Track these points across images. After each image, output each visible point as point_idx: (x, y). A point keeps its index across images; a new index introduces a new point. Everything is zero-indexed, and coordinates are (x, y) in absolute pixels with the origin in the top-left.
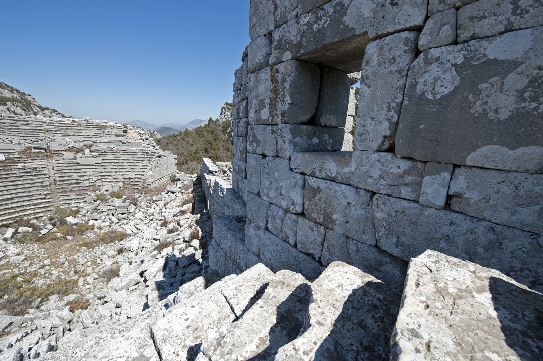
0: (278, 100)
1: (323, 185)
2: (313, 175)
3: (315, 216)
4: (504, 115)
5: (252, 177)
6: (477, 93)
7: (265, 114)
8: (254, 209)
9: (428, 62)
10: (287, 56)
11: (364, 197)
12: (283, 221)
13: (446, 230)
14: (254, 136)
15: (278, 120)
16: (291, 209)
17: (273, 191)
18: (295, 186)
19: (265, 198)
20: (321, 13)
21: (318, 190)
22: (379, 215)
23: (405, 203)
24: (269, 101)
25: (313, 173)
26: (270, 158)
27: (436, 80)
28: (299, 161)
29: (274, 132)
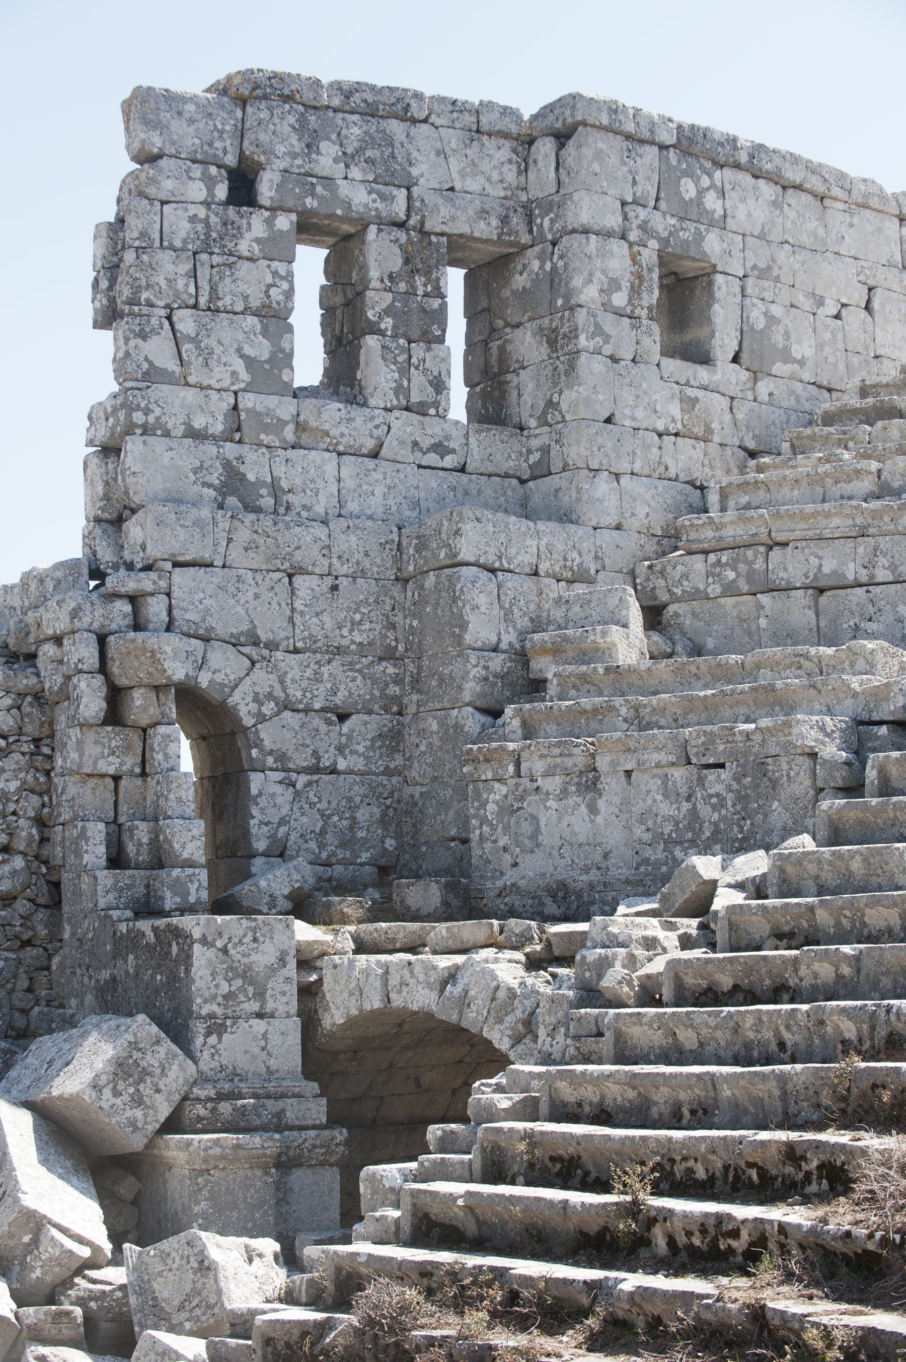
1: (700, 394)
2: (688, 384)
4: (781, 346)
5: (598, 392)
7: (620, 299)
8: (609, 445)
10: (653, 244)
12: (660, 448)
14: (597, 325)
15: (637, 312)
17: (641, 408)
18: (672, 398)
19: (627, 423)
21: (696, 400)
22: (740, 416)
25: (688, 381)
28: (671, 368)
29: (633, 327)
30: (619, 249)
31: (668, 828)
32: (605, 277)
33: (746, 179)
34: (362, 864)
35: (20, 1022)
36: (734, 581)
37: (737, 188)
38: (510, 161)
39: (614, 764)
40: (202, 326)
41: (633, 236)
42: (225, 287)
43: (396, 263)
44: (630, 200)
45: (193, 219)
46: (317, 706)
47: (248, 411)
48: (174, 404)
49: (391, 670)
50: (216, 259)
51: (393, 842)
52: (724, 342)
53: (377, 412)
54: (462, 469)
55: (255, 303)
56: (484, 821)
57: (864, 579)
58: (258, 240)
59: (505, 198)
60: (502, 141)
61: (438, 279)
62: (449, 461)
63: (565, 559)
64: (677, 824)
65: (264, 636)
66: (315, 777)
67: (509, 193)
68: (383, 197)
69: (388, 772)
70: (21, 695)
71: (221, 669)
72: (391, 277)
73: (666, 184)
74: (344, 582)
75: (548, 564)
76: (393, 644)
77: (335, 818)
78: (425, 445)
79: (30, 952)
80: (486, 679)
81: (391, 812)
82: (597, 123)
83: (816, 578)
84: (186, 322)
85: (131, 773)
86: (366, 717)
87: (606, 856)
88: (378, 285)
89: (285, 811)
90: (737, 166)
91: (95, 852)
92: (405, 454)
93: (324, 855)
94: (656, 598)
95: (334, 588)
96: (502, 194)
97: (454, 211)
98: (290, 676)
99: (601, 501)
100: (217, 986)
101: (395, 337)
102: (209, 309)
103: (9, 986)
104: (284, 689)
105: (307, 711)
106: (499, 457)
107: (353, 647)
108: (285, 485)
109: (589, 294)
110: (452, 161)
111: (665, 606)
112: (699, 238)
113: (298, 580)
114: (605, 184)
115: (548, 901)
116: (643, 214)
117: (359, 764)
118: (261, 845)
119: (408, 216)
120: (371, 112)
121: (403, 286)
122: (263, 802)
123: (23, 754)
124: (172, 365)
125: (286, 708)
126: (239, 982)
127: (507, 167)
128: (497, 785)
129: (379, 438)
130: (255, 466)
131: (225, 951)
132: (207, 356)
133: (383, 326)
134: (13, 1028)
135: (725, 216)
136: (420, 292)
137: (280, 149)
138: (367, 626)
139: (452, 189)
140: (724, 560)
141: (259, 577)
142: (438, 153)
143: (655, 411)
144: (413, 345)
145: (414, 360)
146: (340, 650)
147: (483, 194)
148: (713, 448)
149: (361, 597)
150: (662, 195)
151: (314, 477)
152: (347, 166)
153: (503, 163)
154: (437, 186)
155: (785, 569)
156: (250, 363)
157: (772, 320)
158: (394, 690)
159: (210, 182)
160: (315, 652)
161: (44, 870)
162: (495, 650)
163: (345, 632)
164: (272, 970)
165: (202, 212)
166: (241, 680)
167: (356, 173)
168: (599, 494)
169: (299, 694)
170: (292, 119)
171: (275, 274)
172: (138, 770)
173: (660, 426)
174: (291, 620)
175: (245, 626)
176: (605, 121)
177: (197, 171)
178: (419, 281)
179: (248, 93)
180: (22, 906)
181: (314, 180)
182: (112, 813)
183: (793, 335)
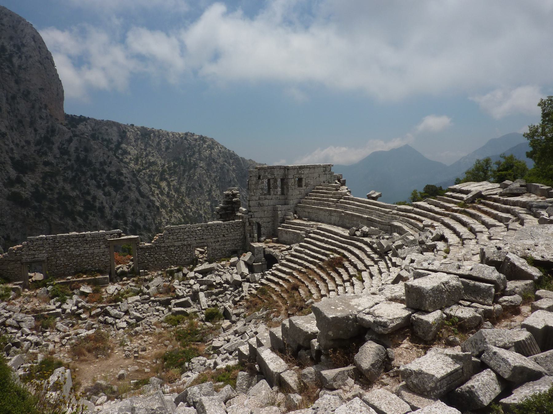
30: (293, 180)
32: (292, 182)
48: (254, 198)
52: (304, 184)
71: (259, 220)
73: (298, 172)
84: (255, 191)
91: (249, 236)
109: (290, 184)
151: (266, 202)
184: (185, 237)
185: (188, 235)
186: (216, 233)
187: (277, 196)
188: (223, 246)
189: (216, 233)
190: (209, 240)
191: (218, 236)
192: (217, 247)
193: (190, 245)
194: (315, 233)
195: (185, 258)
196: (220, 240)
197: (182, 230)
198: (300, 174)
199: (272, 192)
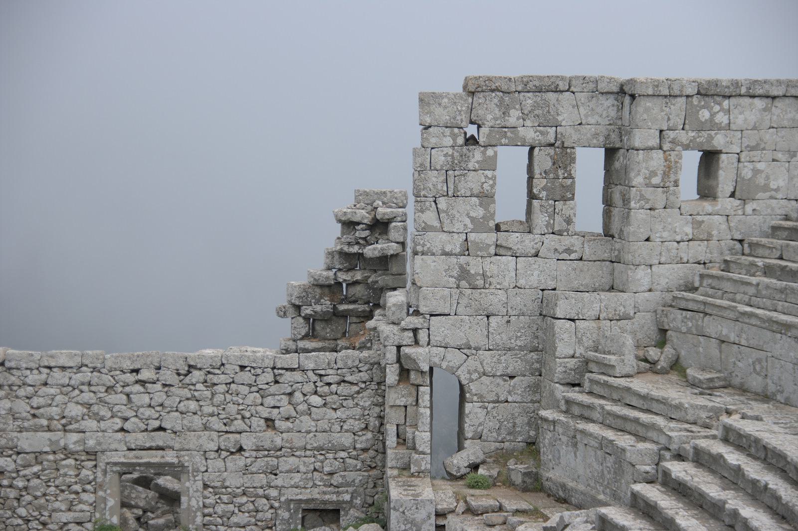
0: (671, 172)
1: (706, 218)
2: (698, 214)
3: (701, 237)
4: (763, 184)
6: (757, 178)
9: (745, 167)
11: (725, 218)
13: (754, 222)
16: (685, 239)
20: (700, 134)
21: (703, 222)
22: (732, 225)
23: (741, 216)
24: (662, 172)
25: (698, 213)
26: (660, 210)
27: (747, 173)
29: (664, 192)
30: (658, 155)
31: (596, 474)
33: (748, 100)
34: (519, 442)
35: (370, 500)
36: (691, 327)
37: (738, 107)
38: (613, 105)
39: (581, 439)
40: (449, 205)
41: (666, 147)
42: (461, 186)
43: (548, 164)
44: (665, 128)
45: (446, 155)
46: (498, 374)
47: (472, 242)
49: (535, 357)
50: (457, 173)
51: (534, 433)
53: (537, 236)
54: (581, 259)
55: (475, 192)
56: (544, 446)
57: (737, 342)
58: (478, 162)
59: (610, 124)
60: (609, 96)
61: (571, 170)
62: (573, 256)
63: (615, 310)
64: (598, 473)
65: (473, 346)
66: (497, 405)
67: (612, 122)
68: (542, 133)
69: (533, 402)
70: (373, 364)
72: (545, 172)
74: (513, 319)
75: (605, 314)
76: (537, 345)
77: (506, 423)
78: (561, 250)
79: (374, 473)
80: (565, 372)
81: (533, 420)
82: (646, 94)
83: (719, 336)
84: (443, 203)
85: (411, 405)
86: (522, 378)
87: (579, 477)
88: (539, 176)
89: (481, 420)
90: (740, 95)
92: (551, 254)
93: (500, 439)
94: (664, 326)
95: (508, 322)
96: (608, 123)
97: (579, 136)
98: (485, 361)
99: (639, 280)
100: (399, 527)
101: (547, 199)
102: (454, 196)
103: (365, 486)
104: (483, 367)
105: (493, 376)
106: (599, 253)
107: (517, 347)
108: (489, 274)
110: (582, 109)
111: (667, 330)
112: (711, 138)
113: (491, 319)
114: (650, 124)
115: (560, 489)
116: (672, 134)
117: (519, 399)
118: (469, 434)
119: (556, 141)
120: (539, 90)
121: (552, 176)
122: (471, 416)
123: (372, 390)
124: (436, 224)
125: (484, 375)
126: (410, 525)
127: (611, 108)
128: (548, 432)
129: (537, 249)
130: (475, 265)
131: (403, 512)
132: (452, 218)
133: (541, 196)
134: (367, 503)
135: (729, 123)
136: (561, 177)
137: (489, 117)
138: (524, 338)
139: (580, 124)
140: (688, 316)
141: (471, 318)
142: (573, 107)
143: (675, 232)
144: (557, 203)
145: (557, 210)
146: (510, 349)
147: (598, 124)
148: (713, 243)
149: (521, 325)
150: (687, 122)
152: (524, 120)
153: (609, 107)
154: (572, 124)
155: (709, 328)
156: (473, 219)
157: (756, 172)
158: (537, 365)
159: (454, 137)
160: (498, 350)
161: (381, 438)
162: (573, 357)
163: (513, 341)
164: (424, 521)
165: (450, 151)
166: (462, 365)
167: (528, 123)
168: (639, 277)
169: (490, 369)
170: (496, 101)
171: (486, 177)
172: (414, 404)
173: (678, 238)
174: (488, 337)
175: (464, 341)
176: (650, 92)
177: (448, 131)
178: (560, 172)
179: (474, 89)
180: (372, 453)
181: (506, 130)
182: (404, 421)
183: (772, 177)
184: (75, 410)
185: (89, 406)
186: (232, 409)
187: (566, 241)
188: (262, 479)
189: (232, 409)
190: (192, 440)
191: (239, 424)
192: (234, 481)
193: (92, 454)
194: (702, 459)
195: (65, 517)
196: (247, 441)
197: (58, 376)
198: (701, 128)
199: (540, 220)
